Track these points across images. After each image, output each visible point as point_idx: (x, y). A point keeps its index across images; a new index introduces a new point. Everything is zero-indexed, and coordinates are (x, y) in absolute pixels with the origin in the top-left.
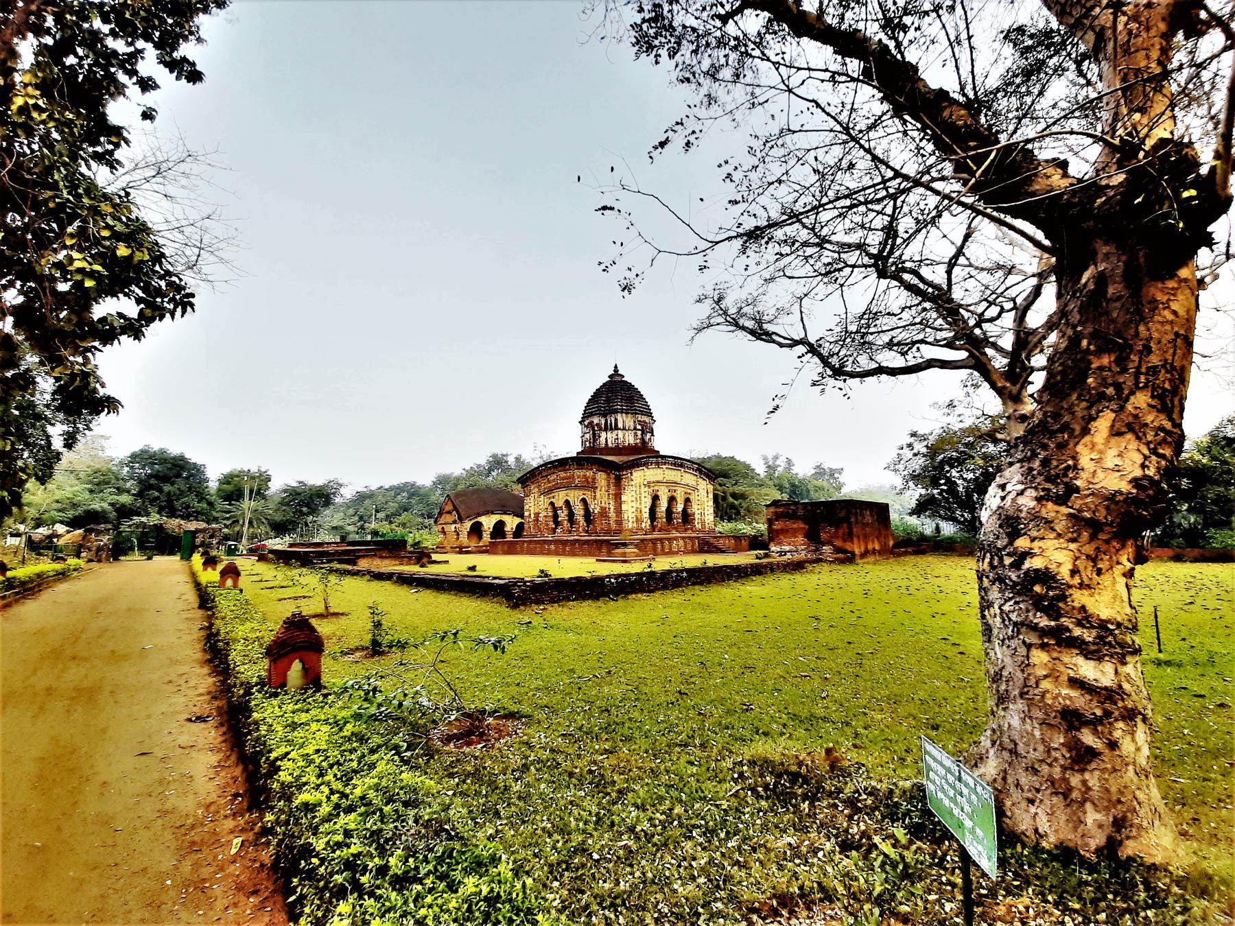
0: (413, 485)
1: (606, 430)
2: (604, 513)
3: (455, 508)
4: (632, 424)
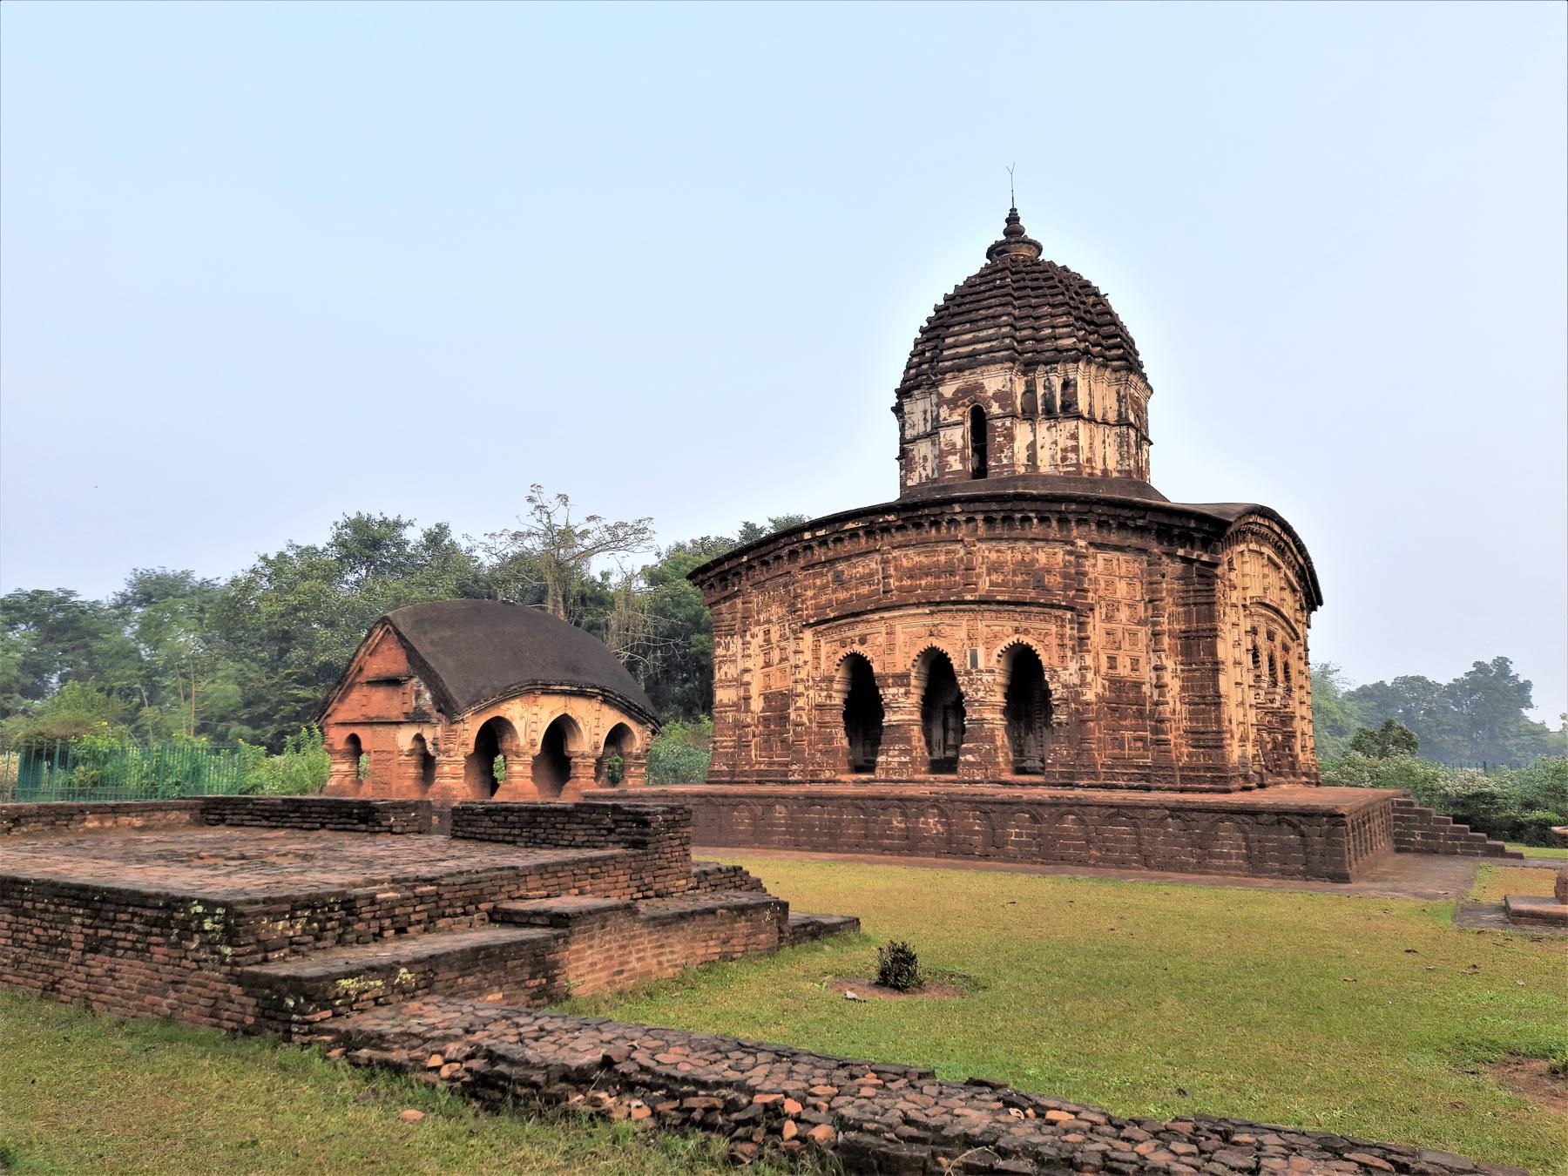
0: (60, 602)
1: (1029, 415)
2: (1125, 697)
3: (418, 664)
4: (1112, 402)
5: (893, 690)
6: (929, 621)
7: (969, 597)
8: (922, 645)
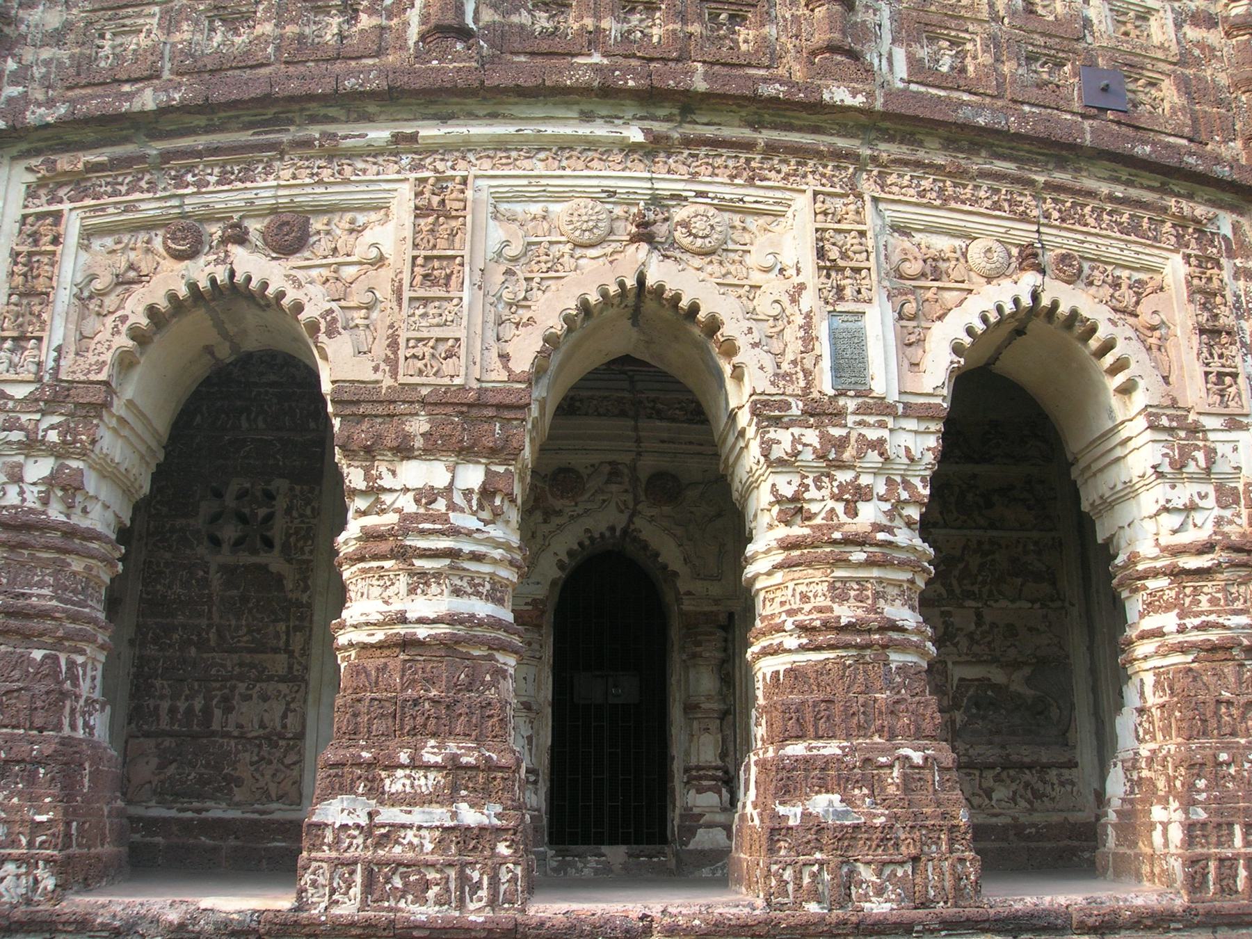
5: (433, 473)
6: (634, 179)
7: (840, 95)
8: (593, 277)
